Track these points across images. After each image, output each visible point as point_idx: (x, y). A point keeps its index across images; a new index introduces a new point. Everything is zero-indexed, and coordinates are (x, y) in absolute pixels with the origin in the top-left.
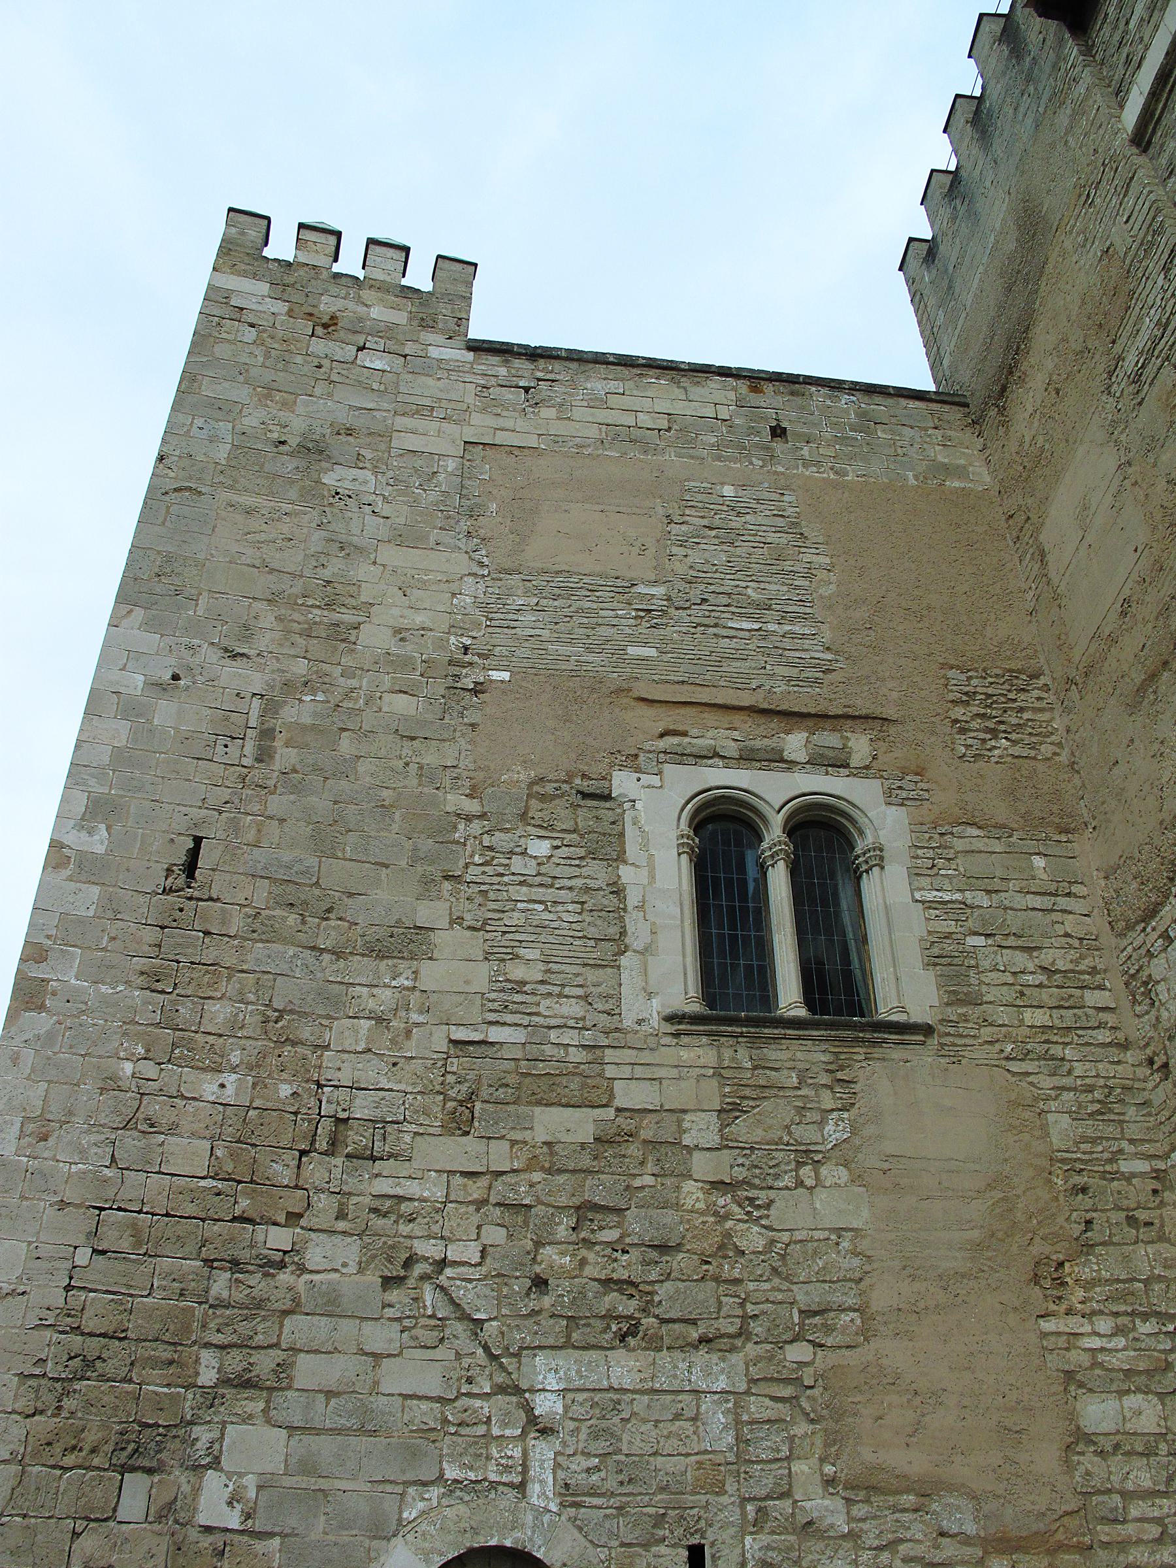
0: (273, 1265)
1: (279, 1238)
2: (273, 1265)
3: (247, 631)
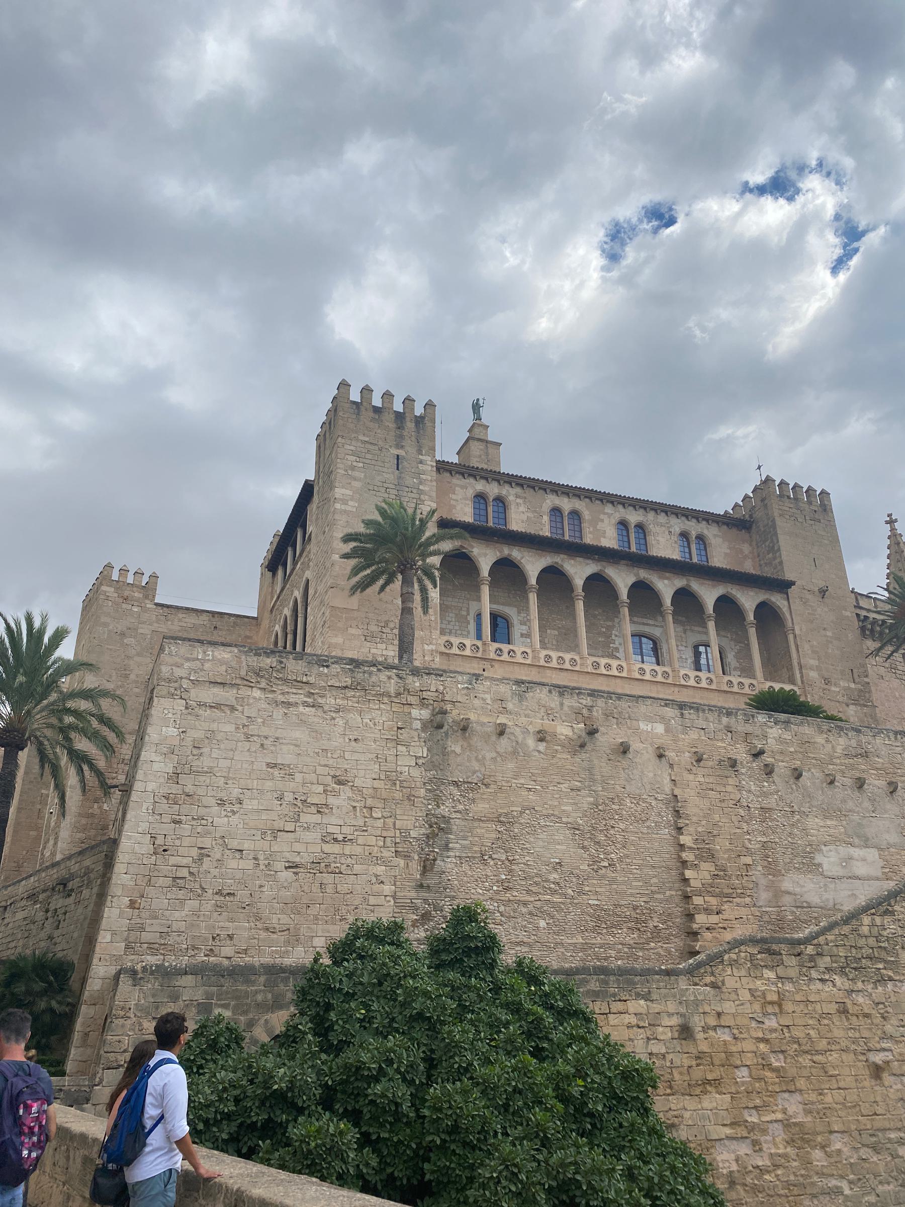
0: (113, 779)
1: (115, 775)
2: (113, 779)
3: (111, 676)
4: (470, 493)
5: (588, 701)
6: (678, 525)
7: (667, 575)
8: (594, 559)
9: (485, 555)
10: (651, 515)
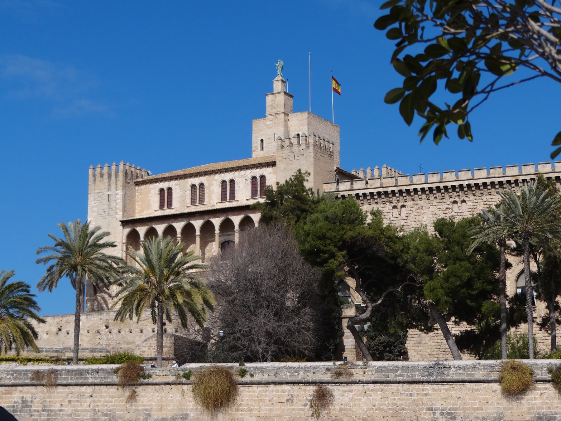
4: (157, 191)
5: (61, 319)
6: (250, 173)
7: (218, 215)
8: (185, 217)
9: (141, 229)
10: (237, 173)
